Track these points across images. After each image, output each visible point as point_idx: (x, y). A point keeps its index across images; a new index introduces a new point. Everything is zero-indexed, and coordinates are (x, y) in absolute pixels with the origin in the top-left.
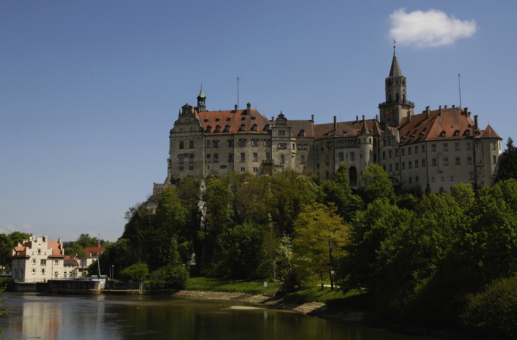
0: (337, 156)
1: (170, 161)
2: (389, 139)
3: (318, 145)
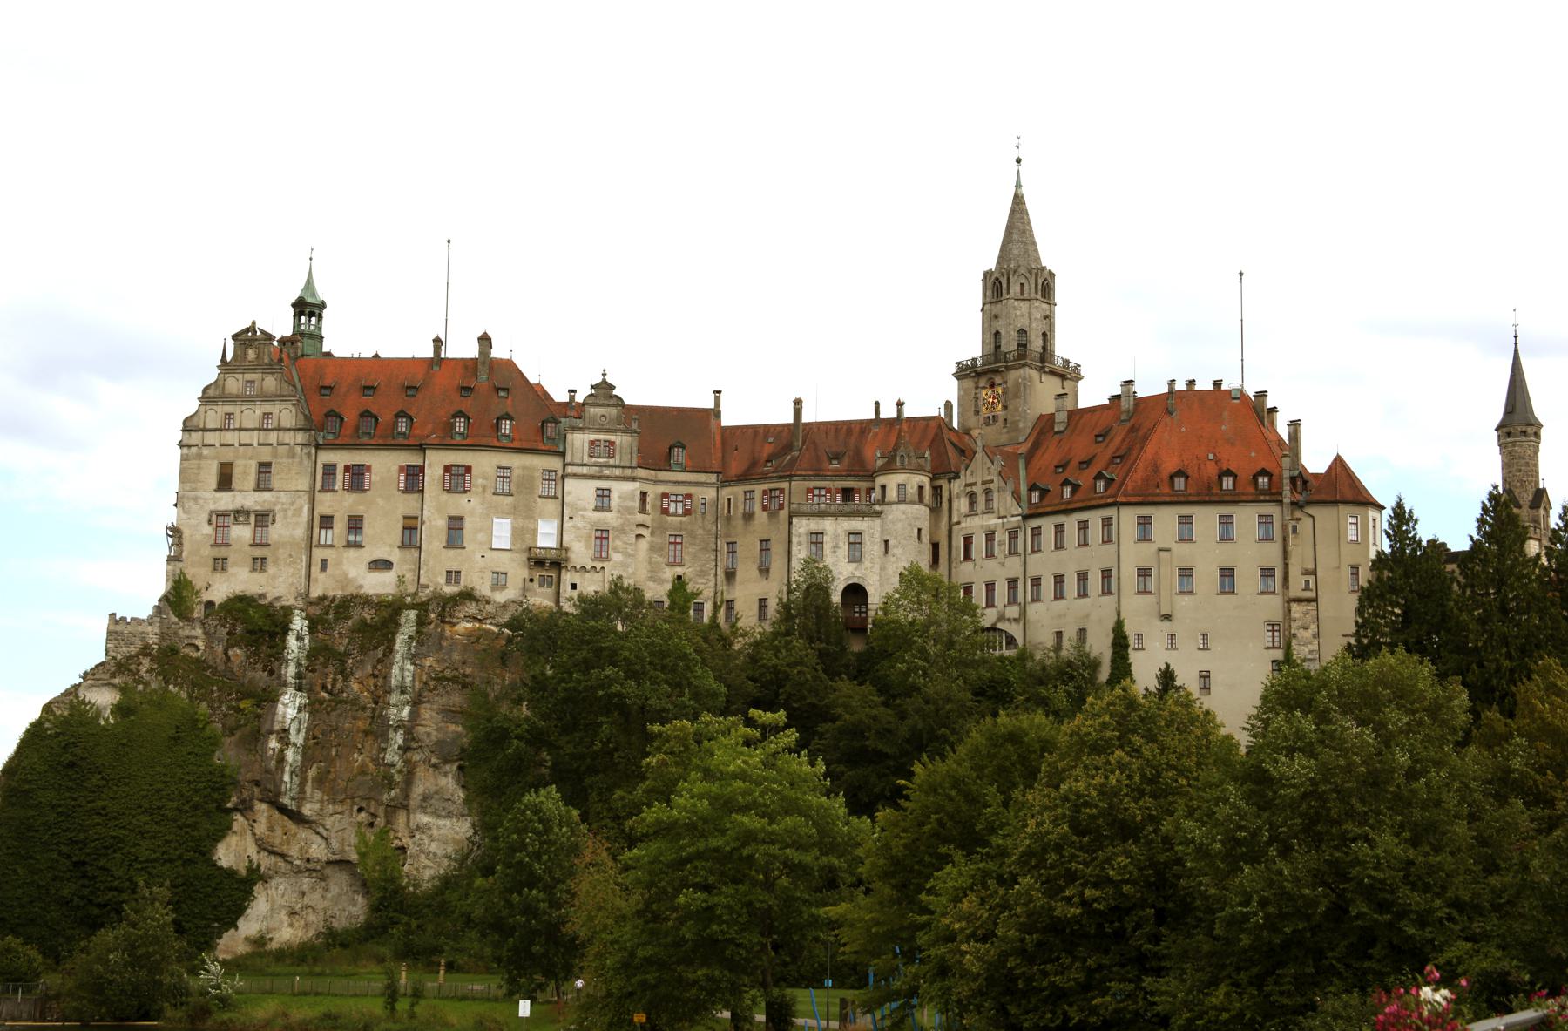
0: (799, 544)
1: (175, 532)
2: (988, 492)
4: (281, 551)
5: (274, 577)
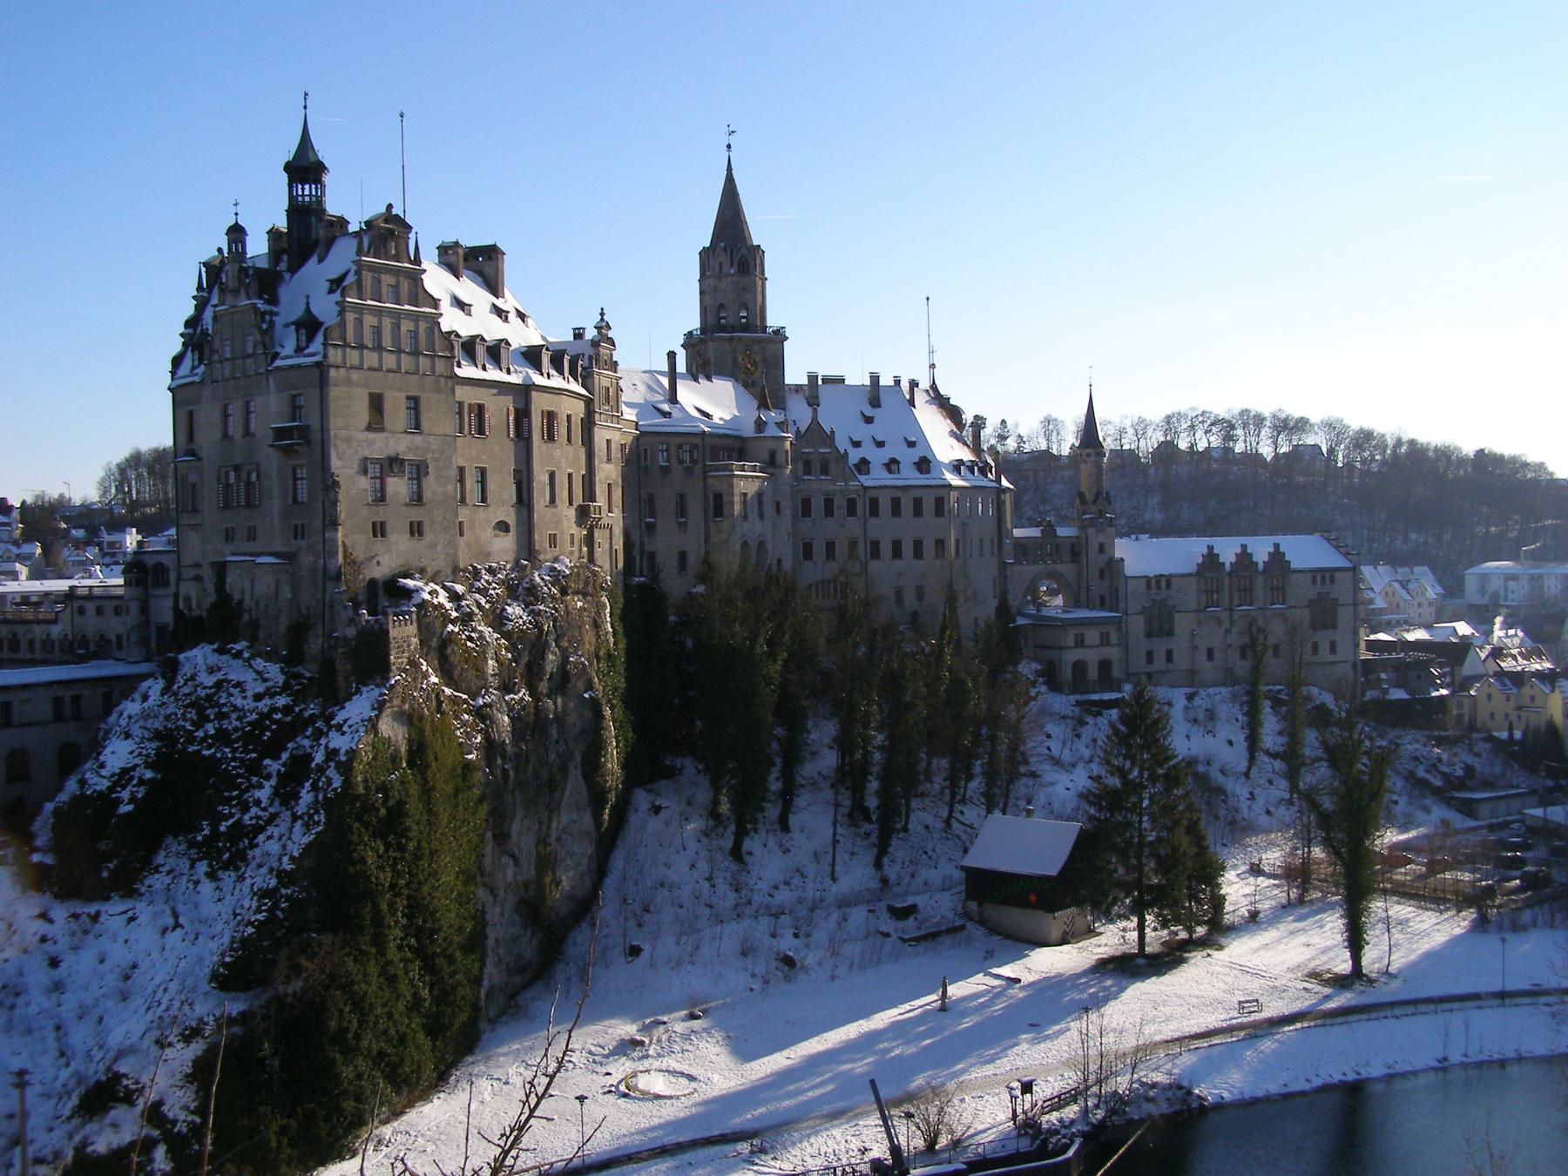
3: (648, 452)
4: (436, 512)
5: (433, 546)
